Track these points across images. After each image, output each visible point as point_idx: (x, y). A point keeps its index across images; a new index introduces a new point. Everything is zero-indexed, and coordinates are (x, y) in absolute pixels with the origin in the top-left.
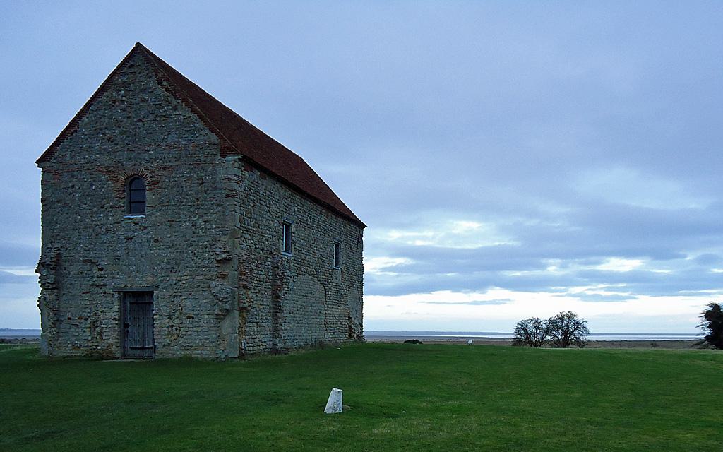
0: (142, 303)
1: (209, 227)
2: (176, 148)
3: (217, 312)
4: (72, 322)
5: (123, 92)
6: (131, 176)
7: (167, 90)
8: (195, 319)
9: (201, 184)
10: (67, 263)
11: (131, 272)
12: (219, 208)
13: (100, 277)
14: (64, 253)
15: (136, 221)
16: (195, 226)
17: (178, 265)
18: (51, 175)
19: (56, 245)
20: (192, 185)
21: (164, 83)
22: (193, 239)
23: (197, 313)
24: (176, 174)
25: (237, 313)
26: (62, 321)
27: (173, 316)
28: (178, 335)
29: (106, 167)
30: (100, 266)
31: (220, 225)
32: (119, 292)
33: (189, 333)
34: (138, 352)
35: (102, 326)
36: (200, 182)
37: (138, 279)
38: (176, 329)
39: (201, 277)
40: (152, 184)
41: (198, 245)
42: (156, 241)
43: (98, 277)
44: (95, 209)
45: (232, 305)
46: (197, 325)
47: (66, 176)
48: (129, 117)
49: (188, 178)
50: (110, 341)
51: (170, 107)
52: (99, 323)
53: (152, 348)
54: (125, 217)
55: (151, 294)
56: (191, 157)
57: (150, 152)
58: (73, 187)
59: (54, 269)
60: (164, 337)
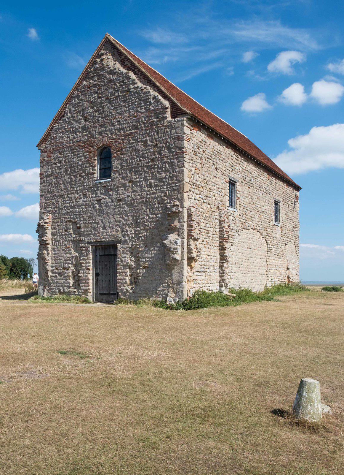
0: (108, 255)
18: (46, 154)
21: (127, 63)
22: (148, 196)
25: (185, 262)
38: (135, 278)
53: (115, 294)
55: (115, 247)
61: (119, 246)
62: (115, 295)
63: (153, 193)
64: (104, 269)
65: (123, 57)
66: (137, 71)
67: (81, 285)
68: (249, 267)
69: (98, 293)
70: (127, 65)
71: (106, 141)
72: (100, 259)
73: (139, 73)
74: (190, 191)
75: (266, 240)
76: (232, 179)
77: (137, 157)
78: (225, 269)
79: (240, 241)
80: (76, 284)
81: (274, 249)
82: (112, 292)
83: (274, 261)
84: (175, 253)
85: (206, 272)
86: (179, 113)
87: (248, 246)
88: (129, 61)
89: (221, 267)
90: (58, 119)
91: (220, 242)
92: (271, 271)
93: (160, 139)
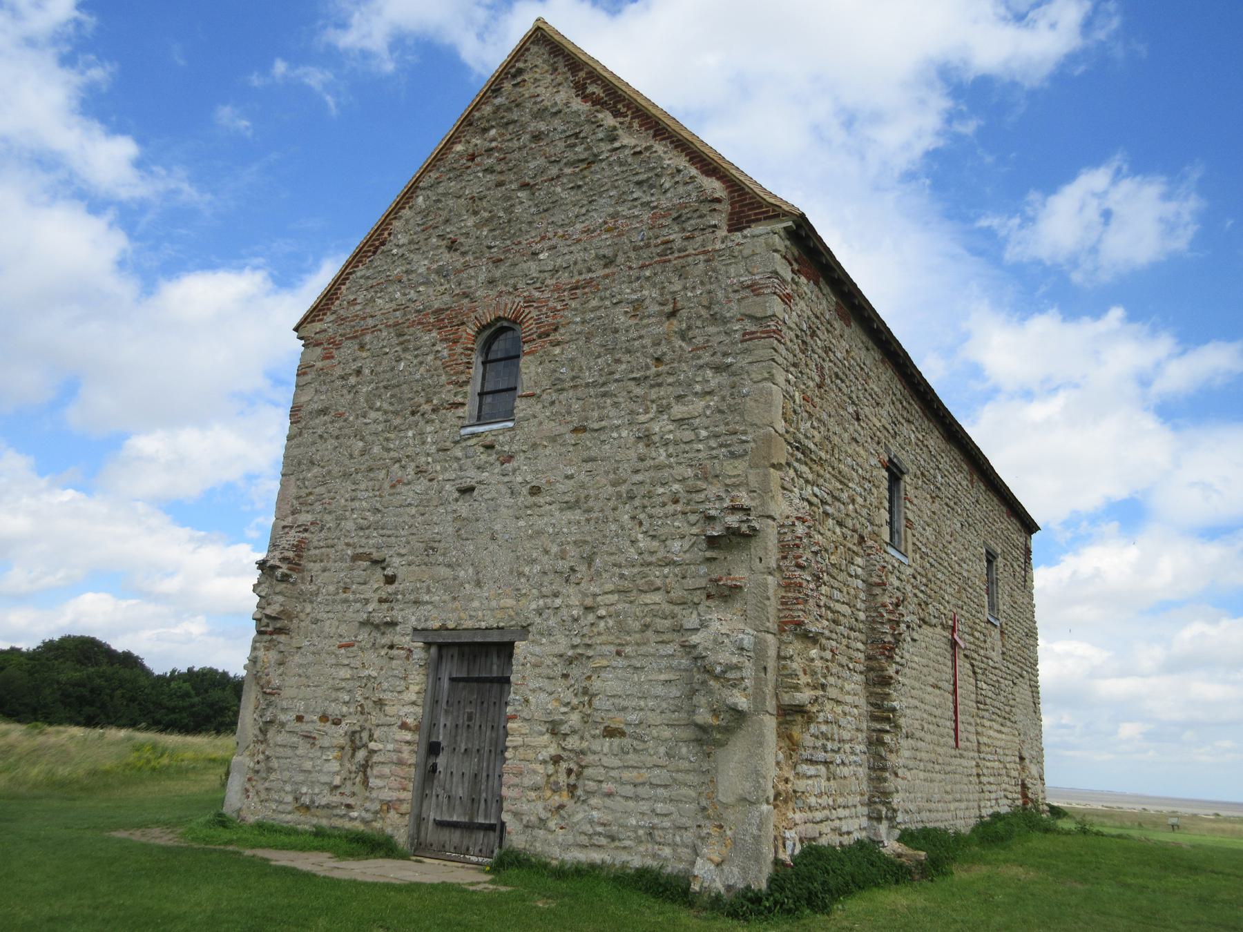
1: (689, 435)
2: (607, 231)
3: (703, 716)
4: (304, 727)
5: (493, 132)
6: (489, 325)
7: (596, 101)
8: (626, 741)
9: (673, 314)
10: (318, 566)
11: (462, 584)
12: (723, 378)
13: (386, 601)
14: (314, 538)
15: (490, 439)
16: (646, 438)
17: (590, 560)
19: (305, 518)
20: (645, 321)
21: (592, 89)
22: (639, 477)
23: (633, 717)
24: (602, 299)
25: (770, 723)
26: (283, 725)
27: (562, 722)
28: (572, 788)
29: (434, 313)
30: (389, 572)
31: (722, 429)
32: (428, 645)
33: (606, 787)
34: (456, 836)
35: (372, 745)
36: (669, 308)
37: (476, 604)
38: (569, 772)
39: (656, 597)
40: (540, 337)
41: (649, 495)
42: (535, 491)
43: (381, 601)
44: (397, 421)
45: (758, 697)
46: (632, 758)
47: (349, 349)
48: (500, 184)
49: (638, 305)
50: (387, 795)
51: (601, 135)
52: (365, 735)
53: (491, 828)
54: (463, 432)
55: (505, 650)
56: (648, 246)
57: (541, 256)
58: (359, 372)
59: (285, 578)
60: (533, 794)
61: (520, 647)
62: (492, 834)
63: (658, 468)
64: (460, 731)
65: (582, 74)
66: (624, 106)
67: (373, 782)
68: (939, 750)
69: (432, 818)
70: (594, 93)
71: (509, 306)
72: (451, 690)
73: (629, 113)
74: (789, 464)
75: (973, 665)
76: (895, 460)
77: (607, 350)
78: (889, 756)
79: (916, 659)
80: (358, 779)
81: (990, 694)
82: (481, 820)
83: (991, 733)
84: (734, 686)
85: (831, 763)
86: (756, 214)
87: (933, 680)
88: (599, 82)
89: (875, 742)
90: (369, 251)
91: (869, 658)
92: (988, 764)
93: (689, 294)
